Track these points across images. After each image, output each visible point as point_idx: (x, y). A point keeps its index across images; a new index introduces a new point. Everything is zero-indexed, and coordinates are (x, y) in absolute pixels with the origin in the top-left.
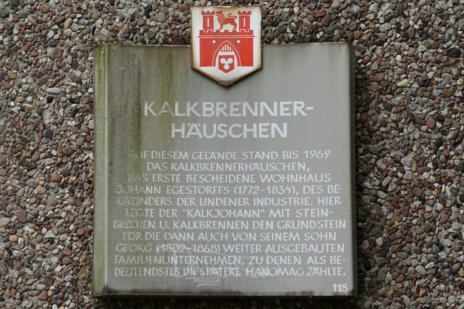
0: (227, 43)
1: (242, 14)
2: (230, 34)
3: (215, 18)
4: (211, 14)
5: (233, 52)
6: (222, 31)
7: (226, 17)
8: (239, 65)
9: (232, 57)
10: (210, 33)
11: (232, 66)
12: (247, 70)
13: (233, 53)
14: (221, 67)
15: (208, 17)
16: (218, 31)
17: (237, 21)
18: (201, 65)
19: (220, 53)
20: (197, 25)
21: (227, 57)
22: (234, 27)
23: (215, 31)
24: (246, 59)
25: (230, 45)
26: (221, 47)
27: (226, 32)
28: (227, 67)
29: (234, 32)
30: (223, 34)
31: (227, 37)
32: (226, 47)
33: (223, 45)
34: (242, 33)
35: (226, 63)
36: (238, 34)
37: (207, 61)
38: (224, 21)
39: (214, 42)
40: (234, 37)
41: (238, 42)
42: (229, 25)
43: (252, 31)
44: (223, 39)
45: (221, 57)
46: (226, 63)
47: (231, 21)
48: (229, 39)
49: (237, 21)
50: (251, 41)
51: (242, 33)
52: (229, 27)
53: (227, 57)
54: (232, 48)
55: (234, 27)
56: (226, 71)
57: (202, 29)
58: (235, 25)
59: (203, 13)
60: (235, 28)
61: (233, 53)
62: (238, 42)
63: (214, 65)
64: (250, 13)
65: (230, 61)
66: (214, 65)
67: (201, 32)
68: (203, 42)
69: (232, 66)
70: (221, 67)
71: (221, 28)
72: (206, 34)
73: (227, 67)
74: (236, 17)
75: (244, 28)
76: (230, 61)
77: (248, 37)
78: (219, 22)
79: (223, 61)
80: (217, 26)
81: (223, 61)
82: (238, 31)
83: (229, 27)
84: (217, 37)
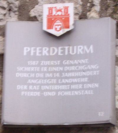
3: (54, 9)
6: (56, 15)
7: (58, 9)
10: (51, 16)
12: (66, 30)
14: (56, 29)
15: (50, 9)
16: (55, 15)
17: (63, 10)
19: (56, 24)
26: (55, 22)
27: (58, 15)
28: (58, 29)
29: (62, 15)
32: (58, 21)
33: (56, 21)
36: (63, 15)
37: (50, 27)
39: (53, 19)
43: (69, 15)
44: (57, 18)
47: (60, 10)
49: (63, 10)
52: (59, 13)
56: (58, 31)
60: (62, 13)
61: (61, 24)
62: (63, 19)
64: (68, 7)
65: (60, 27)
67: (48, 16)
70: (56, 29)
71: (56, 14)
73: (58, 29)
74: (62, 9)
76: (60, 27)
77: (68, 16)
79: (57, 27)
80: (54, 13)
83: (59, 13)
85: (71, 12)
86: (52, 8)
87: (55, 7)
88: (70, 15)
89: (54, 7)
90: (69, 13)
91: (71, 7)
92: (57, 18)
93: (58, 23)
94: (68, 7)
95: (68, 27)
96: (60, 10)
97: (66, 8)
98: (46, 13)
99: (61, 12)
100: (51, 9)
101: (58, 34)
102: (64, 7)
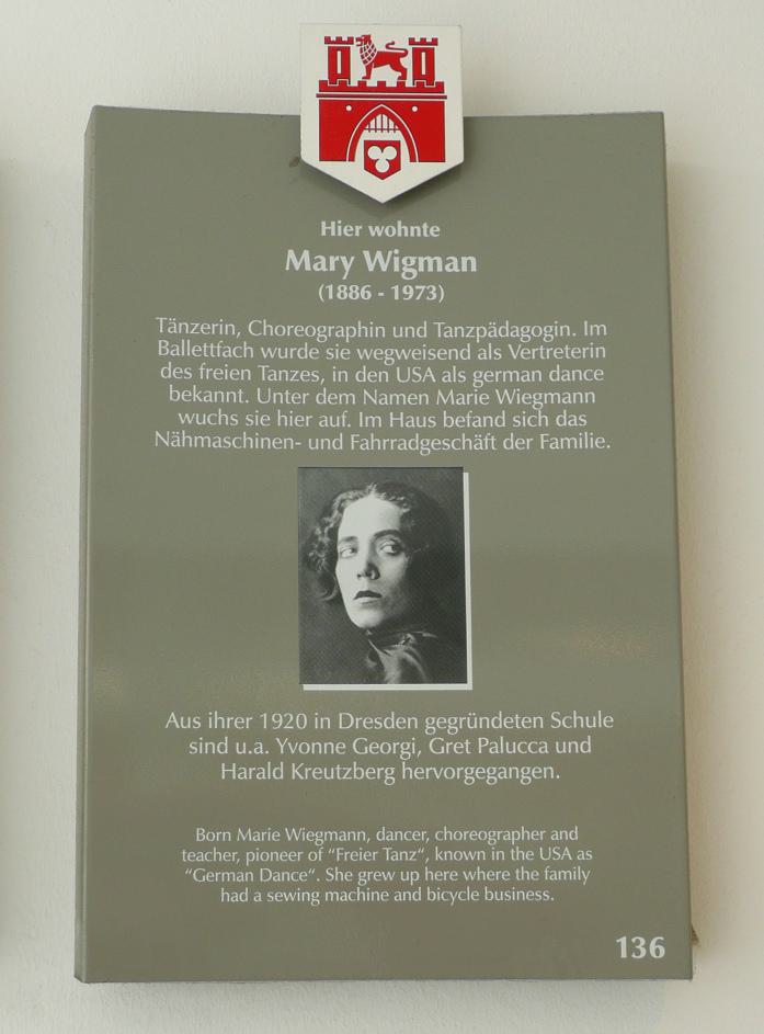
1: (418, 44)
3: (355, 51)
4: (345, 43)
5: (399, 133)
6: (372, 83)
7: (381, 48)
8: (412, 159)
9: (396, 145)
10: (344, 87)
11: (395, 166)
12: (432, 170)
13: (398, 136)
14: (370, 165)
16: (362, 86)
17: (407, 62)
18: (323, 157)
19: (366, 136)
21: (382, 145)
22: (400, 74)
23: (354, 83)
25: (390, 116)
26: (368, 121)
27: (382, 86)
28: (382, 167)
29: (401, 87)
30: (371, 89)
33: (374, 116)
34: (420, 88)
35: (382, 158)
40: (402, 97)
42: (387, 68)
43: (440, 87)
45: (368, 144)
46: (382, 158)
49: (407, 62)
50: (438, 109)
51: (420, 88)
52: (387, 75)
53: (382, 145)
54: (397, 123)
55: (400, 74)
56: (383, 176)
57: (326, 78)
58: (404, 71)
59: (327, 40)
60: (404, 77)
63: (352, 159)
64: (435, 42)
65: (390, 153)
66: (352, 159)
67: (323, 86)
69: (395, 166)
70: (370, 165)
71: (368, 77)
73: (382, 167)
75: (422, 77)
76: (390, 153)
78: (365, 62)
79: (374, 152)
80: (357, 72)
81: (374, 152)
83: (387, 75)
86: (350, 41)
87: (367, 39)
89: (358, 39)
93: (382, 129)
94: (435, 42)
95: (441, 158)
96: (390, 59)
99: (397, 67)
102: (412, 42)
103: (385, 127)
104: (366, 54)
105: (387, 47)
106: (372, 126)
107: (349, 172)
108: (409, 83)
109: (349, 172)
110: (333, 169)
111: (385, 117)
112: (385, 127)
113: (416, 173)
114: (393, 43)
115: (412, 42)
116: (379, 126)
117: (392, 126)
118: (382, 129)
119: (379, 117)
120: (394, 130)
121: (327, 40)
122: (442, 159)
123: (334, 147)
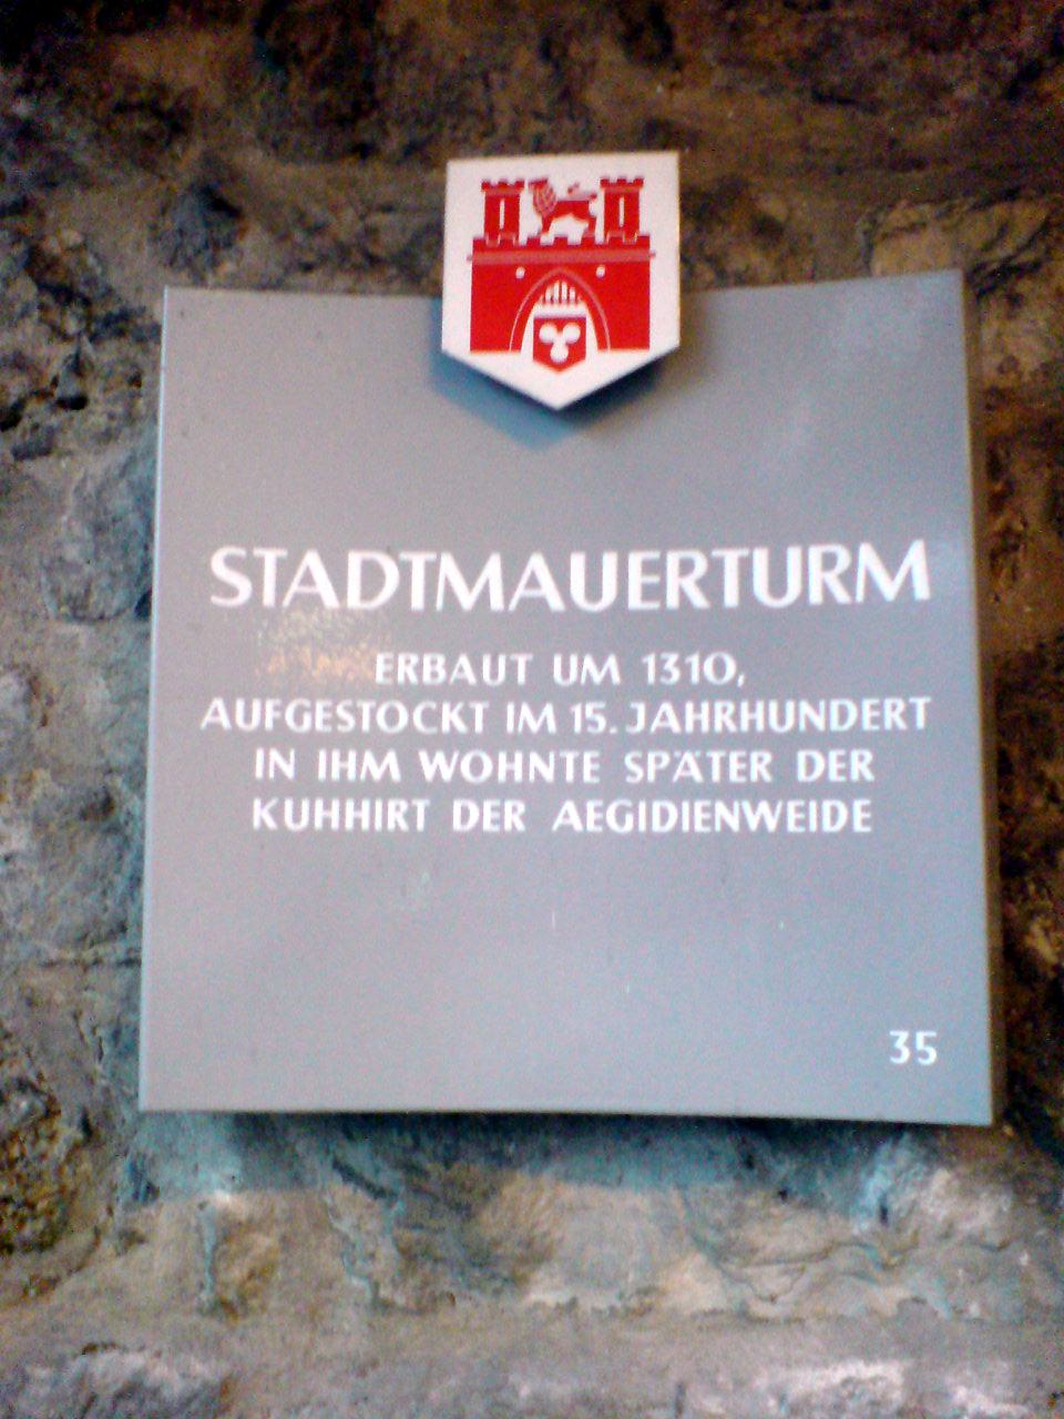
0: (560, 277)
2: (575, 247)
3: (526, 199)
6: (547, 239)
7: (561, 193)
8: (602, 345)
9: (581, 322)
10: (507, 246)
12: (627, 361)
13: (581, 309)
14: (542, 352)
16: (533, 243)
19: (539, 310)
20: (464, 222)
21: (560, 323)
22: (584, 225)
23: (523, 239)
24: (627, 326)
25: (571, 283)
26: (542, 290)
27: (561, 242)
28: (559, 353)
29: (588, 242)
30: (547, 248)
31: (563, 256)
33: (551, 282)
34: (614, 243)
36: (601, 247)
38: (553, 210)
41: (601, 271)
43: (644, 242)
44: (548, 264)
45: (539, 323)
47: (578, 208)
48: (569, 266)
49: (597, 208)
53: (560, 323)
54: (580, 291)
56: (560, 367)
58: (592, 222)
59: (486, 186)
63: (517, 346)
64: (639, 182)
65: (572, 333)
67: (478, 245)
68: (480, 274)
69: (577, 352)
71: (546, 227)
72: (493, 250)
73: (559, 353)
74: (594, 196)
76: (572, 333)
78: (539, 212)
79: (548, 333)
80: (529, 223)
81: (548, 333)
82: (600, 235)
84: (535, 257)
85: (661, 220)
86: (520, 185)
87: (540, 184)
88: (654, 246)
89: (531, 184)
90: (646, 225)
91: (659, 179)
92: (550, 266)
93: (559, 302)
94: (639, 182)
96: (578, 208)
97: (623, 195)
98: (464, 222)
100: (500, 198)
101: (560, 389)
102: (605, 183)
103: (564, 296)
104: (542, 202)
105: (570, 191)
106: (548, 296)
107: (514, 367)
108: (600, 235)
109: (514, 367)
110: (495, 364)
111: (565, 287)
112: (564, 296)
113: (606, 366)
114: (577, 186)
115: (605, 183)
116: (556, 296)
117: (573, 294)
118: (559, 302)
119: (557, 286)
120: (576, 301)
121: (486, 186)
122: (642, 341)
123: (494, 327)
